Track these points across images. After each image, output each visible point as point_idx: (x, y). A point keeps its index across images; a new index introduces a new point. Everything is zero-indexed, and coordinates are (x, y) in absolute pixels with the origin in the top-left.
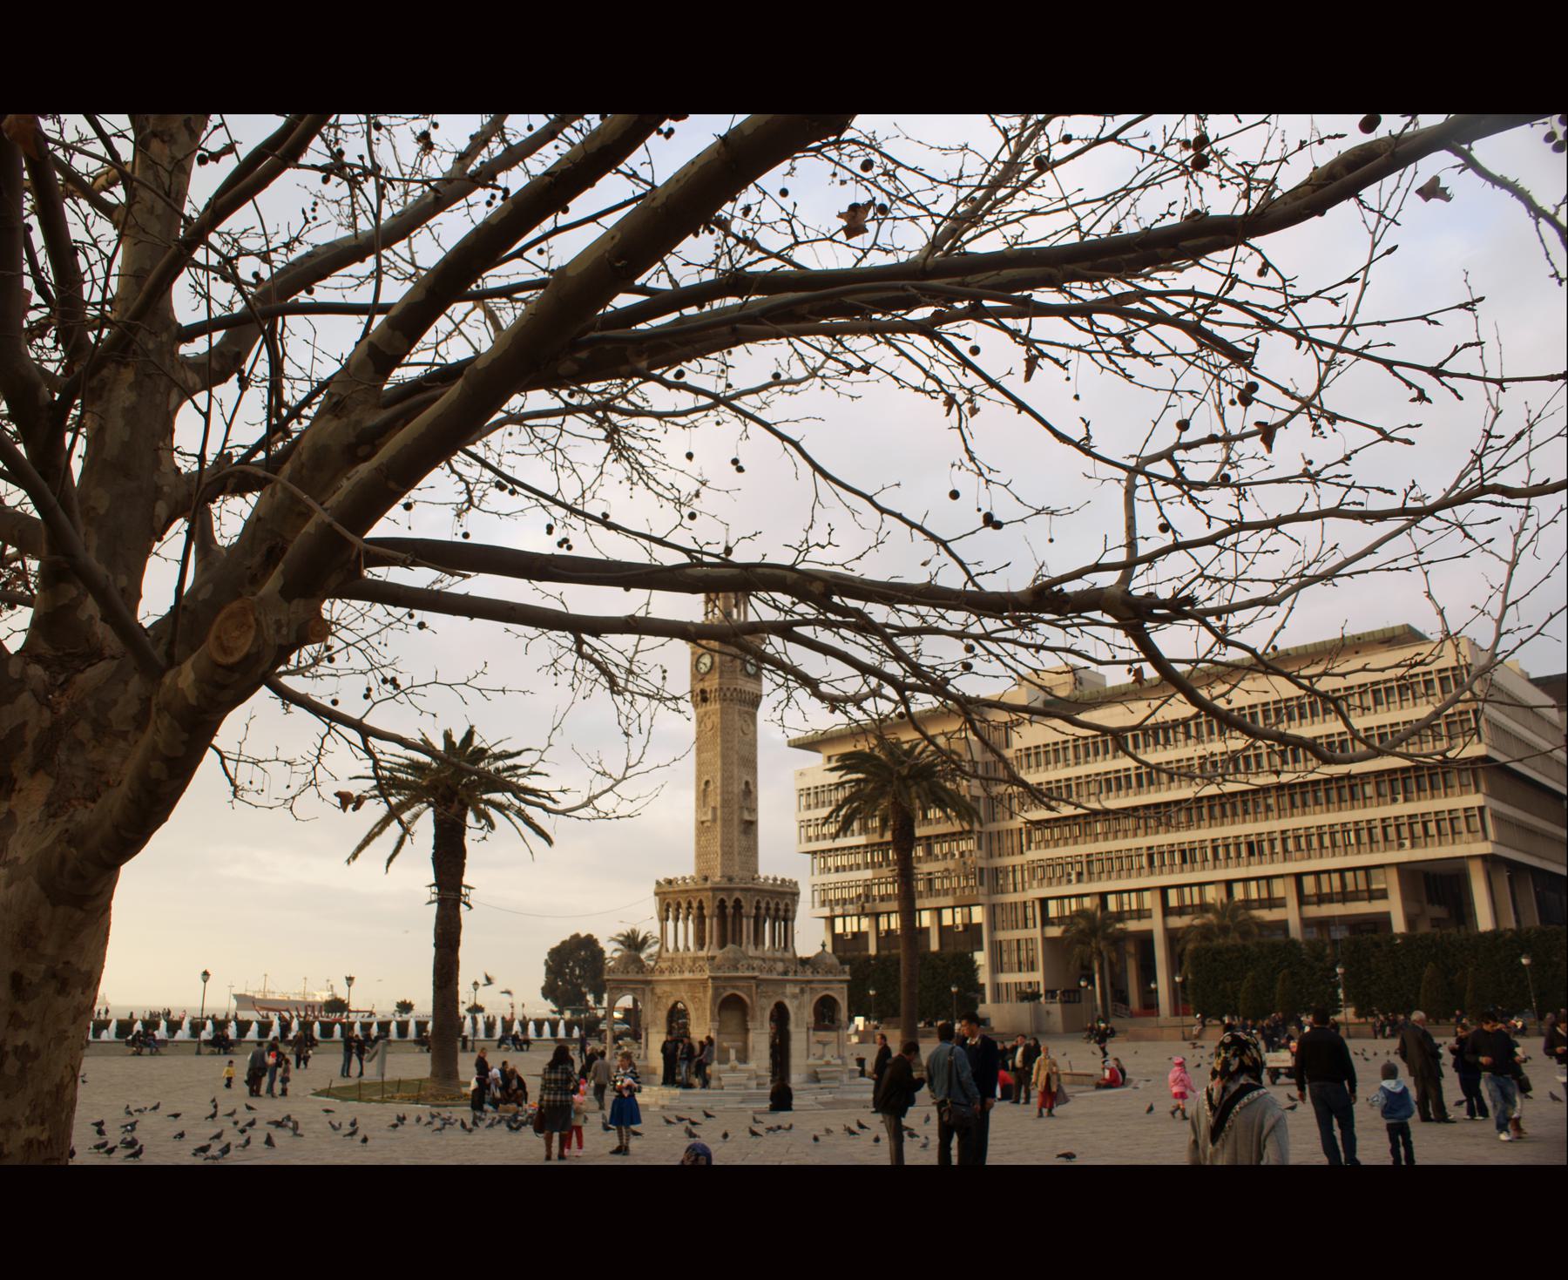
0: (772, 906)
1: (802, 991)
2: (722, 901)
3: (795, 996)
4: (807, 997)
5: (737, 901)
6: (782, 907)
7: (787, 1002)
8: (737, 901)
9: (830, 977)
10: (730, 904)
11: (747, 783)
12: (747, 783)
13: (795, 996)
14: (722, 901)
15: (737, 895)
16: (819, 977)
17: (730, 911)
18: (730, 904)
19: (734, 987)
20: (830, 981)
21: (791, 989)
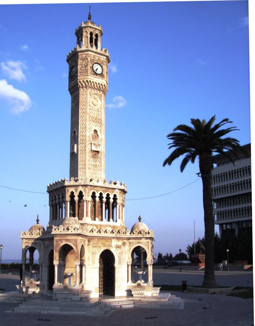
0: (105, 196)
1: (124, 244)
2: (72, 193)
3: (118, 247)
4: (127, 247)
5: (81, 193)
6: (112, 196)
7: (113, 250)
8: (81, 193)
9: (140, 236)
10: (76, 194)
11: (95, 131)
12: (95, 131)
13: (118, 247)
14: (72, 193)
15: (81, 189)
16: (134, 236)
17: (76, 198)
18: (76, 194)
19: (66, 240)
20: (140, 238)
21: (114, 243)
